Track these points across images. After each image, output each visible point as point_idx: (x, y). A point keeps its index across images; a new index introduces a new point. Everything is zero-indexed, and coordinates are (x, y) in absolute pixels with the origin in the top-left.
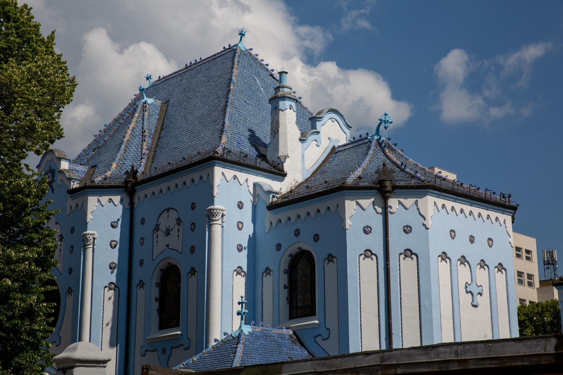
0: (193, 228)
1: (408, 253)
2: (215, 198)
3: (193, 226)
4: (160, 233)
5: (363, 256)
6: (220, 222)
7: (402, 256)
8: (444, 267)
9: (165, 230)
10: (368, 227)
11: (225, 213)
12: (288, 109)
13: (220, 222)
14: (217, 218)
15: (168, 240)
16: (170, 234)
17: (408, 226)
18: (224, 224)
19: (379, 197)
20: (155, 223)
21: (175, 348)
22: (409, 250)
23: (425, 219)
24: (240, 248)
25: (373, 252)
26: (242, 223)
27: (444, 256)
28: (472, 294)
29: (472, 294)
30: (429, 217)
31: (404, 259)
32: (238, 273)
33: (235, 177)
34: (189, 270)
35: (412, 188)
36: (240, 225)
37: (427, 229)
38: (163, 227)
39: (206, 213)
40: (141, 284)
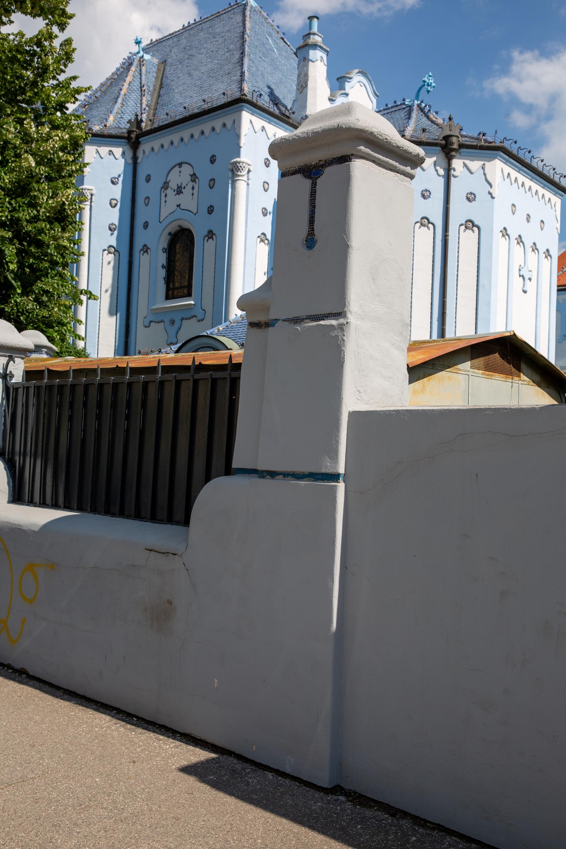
0: (211, 185)
1: (470, 224)
2: (242, 149)
3: (212, 183)
4: (169, 191)
5: (419, 224)
6: (245, 178)
7: (463, 228)
8: (503, 243)
9: (176, 188)
10: (426, 190)
11: (251, 168)
12: (319, 61)
13: (245, 178)
14: (243, 173)
15: (180, 199)
16: (182, 193)
17: (471, 193)
18: (250, 181)
19: (442, 156)
20: (164, 180)
21: (186, 319)
22: (470, 221)
23: (491, 186)
24: (265, 213)
25: (431, 220)
26: (268, 184)
27: (505, 233)
28: (524, 279)
29: (524, 279)
30: (497, 184)
31: (465, 231)
32: (262, 241)
33: (263, 129)
34: (206, 233)
35: (482, 148)
36: (266, 185)
37: (493, 198)
38: (173, 185)
39: (230, 167)
40: (145, 249)
